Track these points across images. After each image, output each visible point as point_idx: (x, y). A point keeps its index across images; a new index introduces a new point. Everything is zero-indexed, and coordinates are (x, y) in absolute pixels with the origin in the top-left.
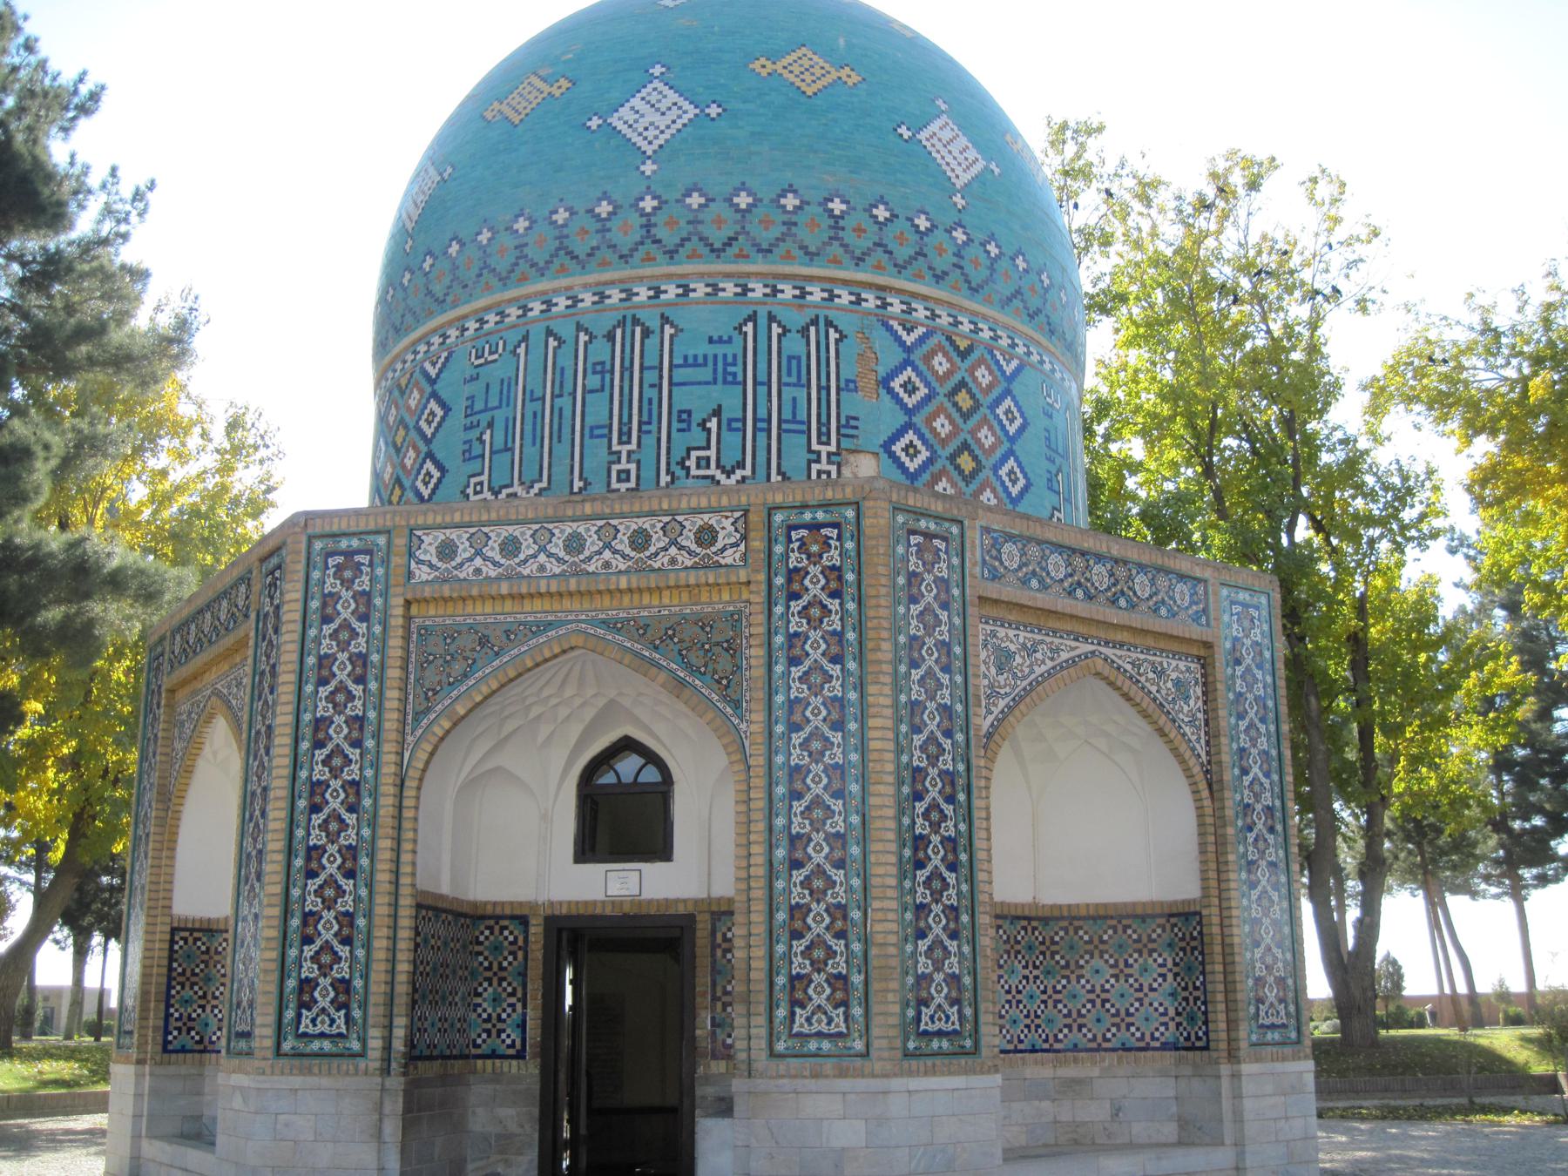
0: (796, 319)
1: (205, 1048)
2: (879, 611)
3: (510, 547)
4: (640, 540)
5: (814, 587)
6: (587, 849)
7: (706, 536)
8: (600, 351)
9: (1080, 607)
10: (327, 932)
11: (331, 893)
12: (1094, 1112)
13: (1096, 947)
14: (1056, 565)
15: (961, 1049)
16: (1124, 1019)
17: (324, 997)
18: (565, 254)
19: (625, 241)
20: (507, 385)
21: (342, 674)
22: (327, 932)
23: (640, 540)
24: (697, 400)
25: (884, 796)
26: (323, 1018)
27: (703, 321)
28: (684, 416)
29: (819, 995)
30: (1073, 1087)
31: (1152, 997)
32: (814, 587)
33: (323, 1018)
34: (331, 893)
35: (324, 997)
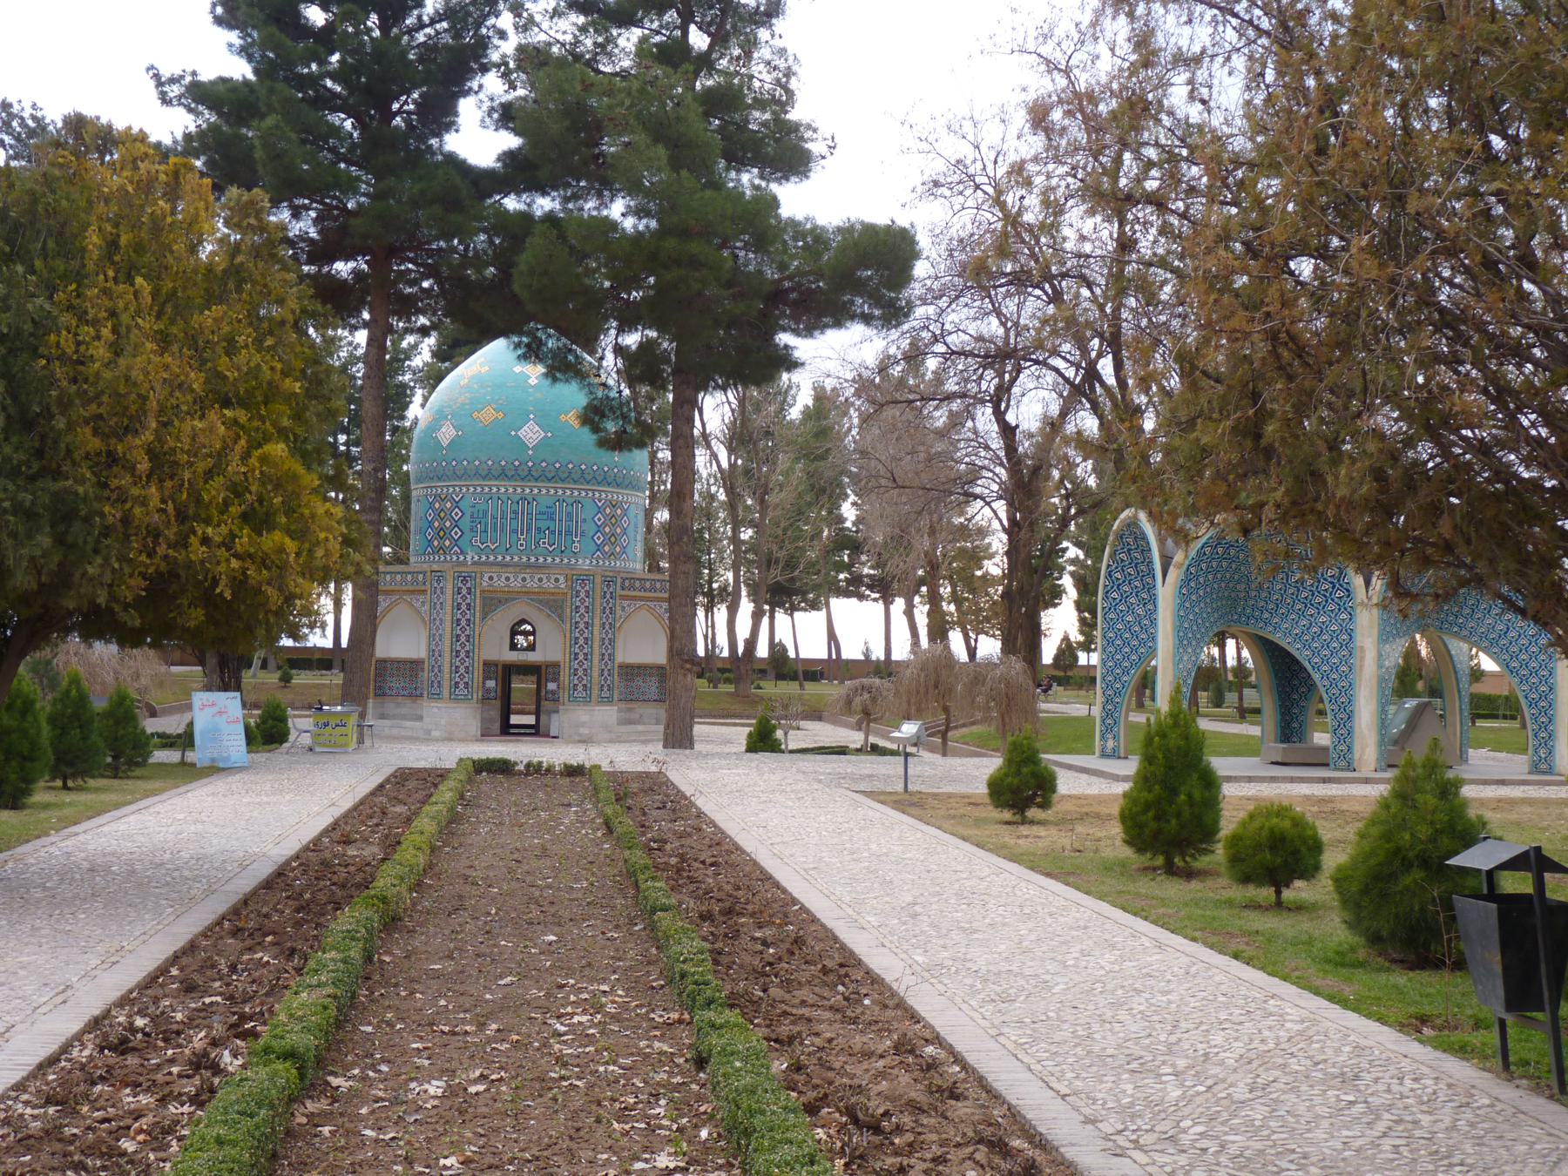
0: (570, 501)
1: (384, 695)
2: (598, 601)
3: (508, 579)
4: (540, 580)
5: (582, 595)
6: (513, 647)
7: (557, 580)
8: (515, 507)
9: (642, 594)
10: (462, 670)
11: (462, 661)
12: (635, 716)
13: (639, 675)
14: (637, 584)
15: (609, 701)
16: (644, 694)
17: (461, 686)
18: (503, 475)
19: (523, 474)
20: (485, 513)
21: (464, 607)
22: (462, 670)
23: (540, 580)
24: (543, 525)
25: (596, 644)
26: (462, 691)
27: (545, 501)
28: (539, 529)
29: (580, 688)
30: (630, 710)
31: (652, 687)
32: (582, 595)
33: (462, 691)
34: (462, 661)
35: (461, 686)
